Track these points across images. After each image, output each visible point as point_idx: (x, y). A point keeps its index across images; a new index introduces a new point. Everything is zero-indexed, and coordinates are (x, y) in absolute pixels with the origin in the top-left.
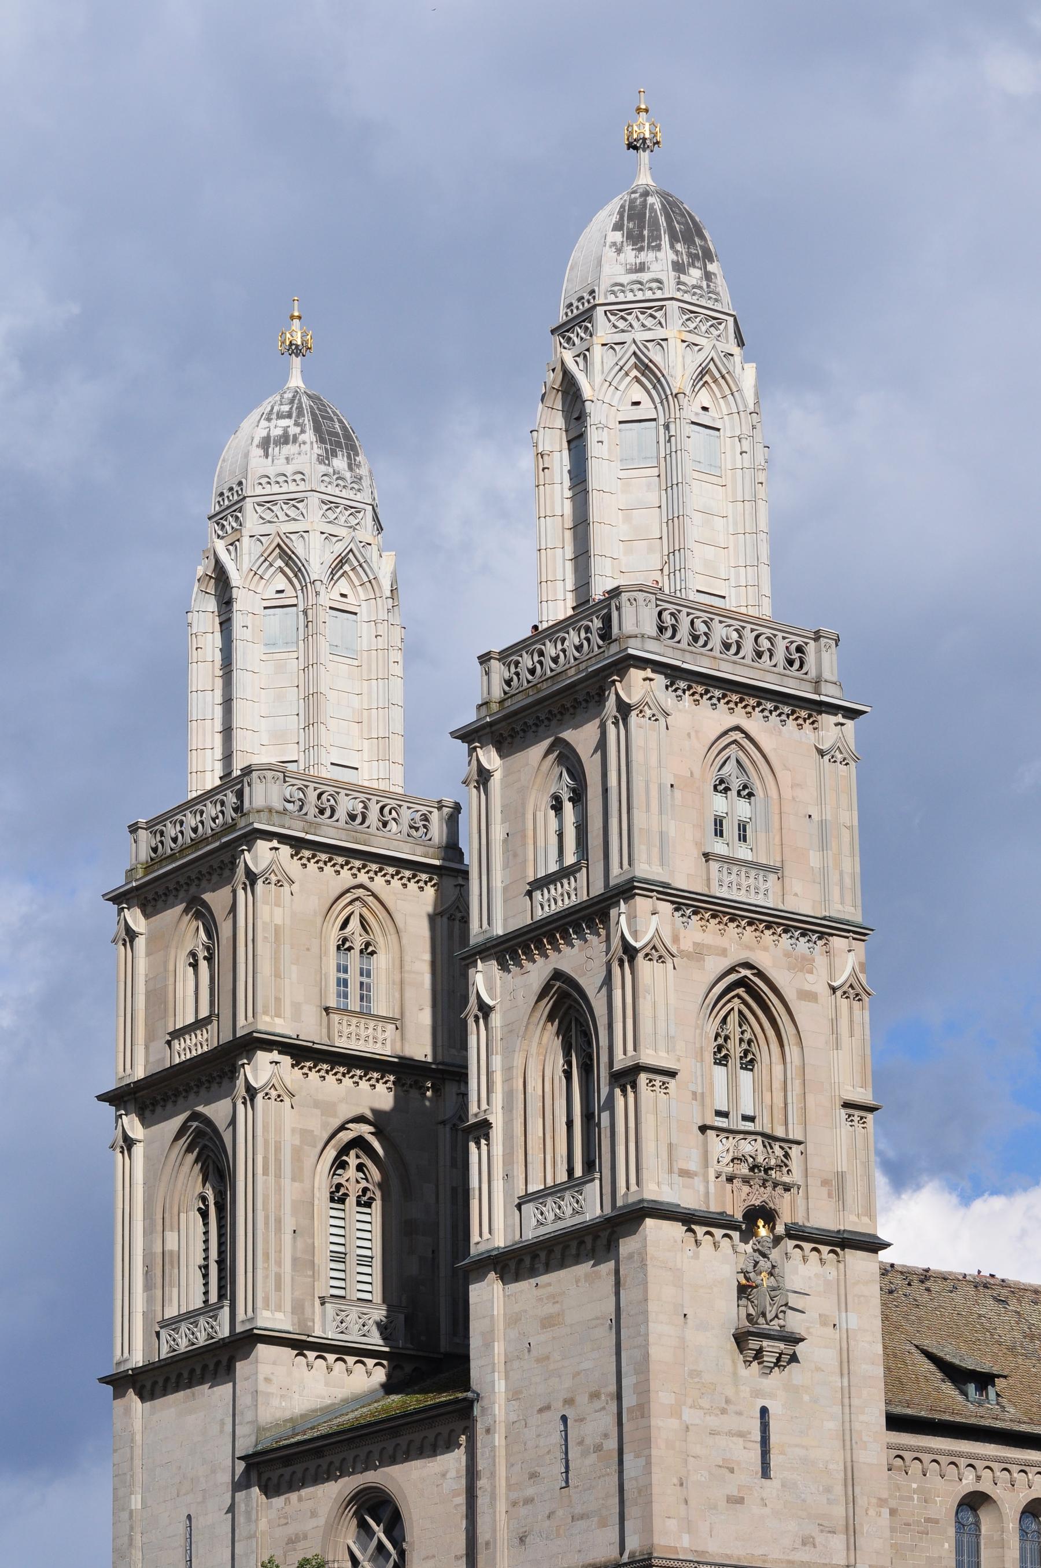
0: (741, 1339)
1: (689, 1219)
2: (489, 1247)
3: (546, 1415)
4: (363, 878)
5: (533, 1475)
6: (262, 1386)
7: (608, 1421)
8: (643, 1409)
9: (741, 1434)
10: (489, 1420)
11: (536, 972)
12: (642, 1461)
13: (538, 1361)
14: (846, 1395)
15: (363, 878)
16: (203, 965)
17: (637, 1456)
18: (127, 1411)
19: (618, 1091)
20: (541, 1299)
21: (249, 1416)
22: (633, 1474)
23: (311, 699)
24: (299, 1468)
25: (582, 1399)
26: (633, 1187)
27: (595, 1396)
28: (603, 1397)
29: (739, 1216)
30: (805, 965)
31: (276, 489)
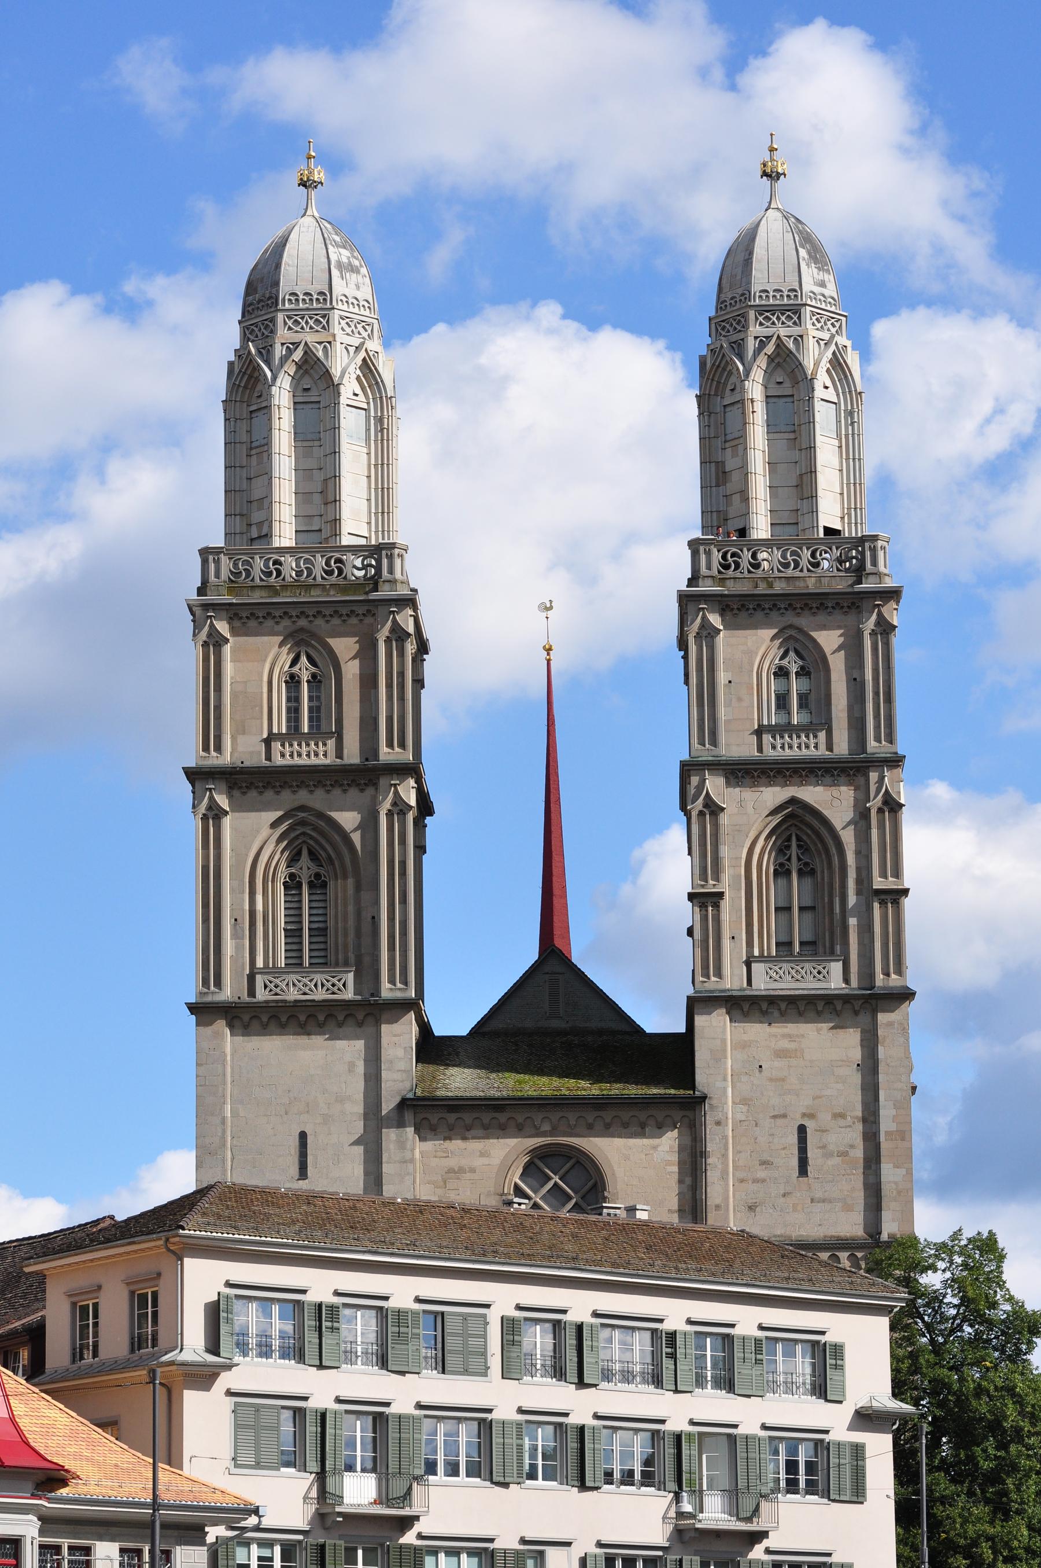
2: (721, 987)
3: (780, 1122)
5: (763, 1163)
8: (903, 1134)
10: (720, 1116)
11: (774, 795)
12: (903, 1171)
13: (771, 1080)
18: (219, 1035)
19: (876, 905)
20: (776, 1036)
24: (468, 1117)
25: (825, 1117)
26: (893, 976)
27: (842, 1116)
28: (849, 1118)
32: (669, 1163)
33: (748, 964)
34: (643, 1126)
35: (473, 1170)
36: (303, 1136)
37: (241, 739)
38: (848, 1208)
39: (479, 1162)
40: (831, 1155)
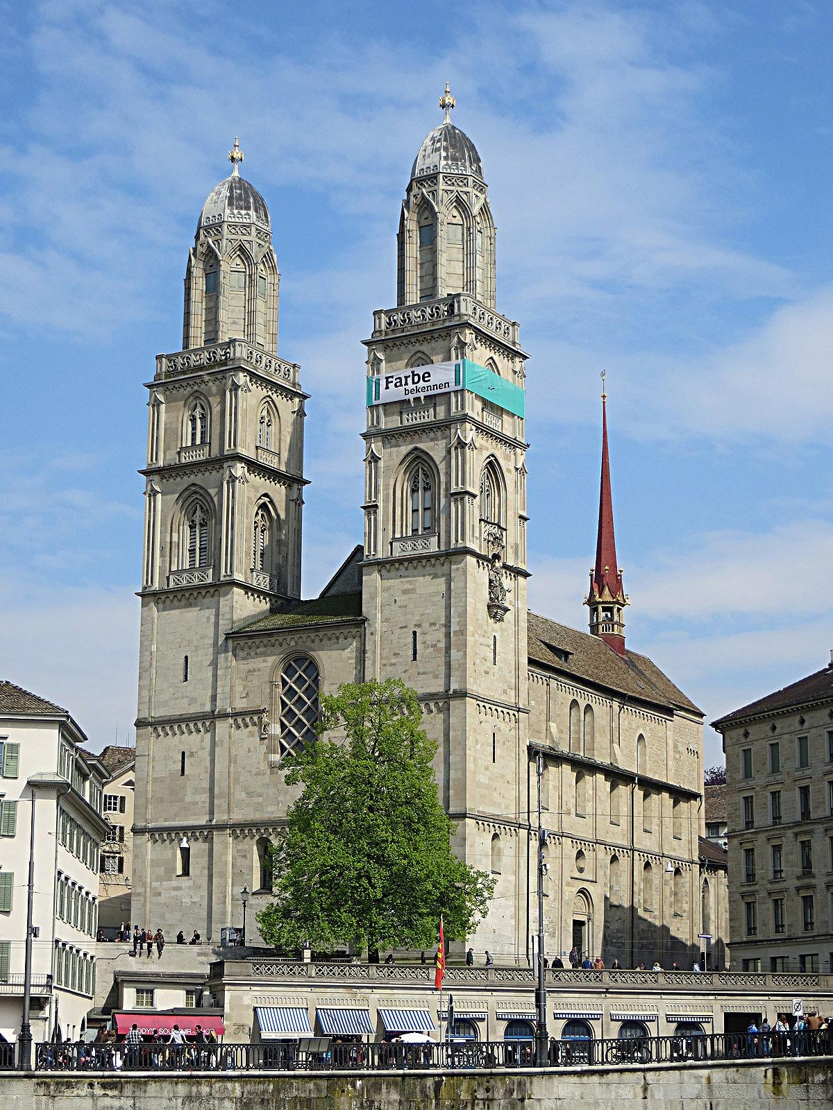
0: (489, 607)
1: (478, 556)
2: (376, 557)
4: (270, 393)
5: (395, 654)
6: (235, 604)
7: (440, 634)
8: (463, 632)
9: (489, 646)
14: (517, 634)
15: (270, 393)
16: (198, 421)
17: (459, 651)
18: (150, 609)
21: (228, 616)
22: (456, 658)
23: (251, 313)
24: (257, 641)
25: (426, 625)
26: (460, 541)
27: (434, 624)
29: (490, 557)
30: (507, 458)
31: (237, 220)
32: (350, 658)
33: (391, 543)
34: (338, 638)
35: (259, 670)
36: (186, 657)
37: (168, 453)
38: (436, 677)
39: (262, 665)
40: (428, 647)
